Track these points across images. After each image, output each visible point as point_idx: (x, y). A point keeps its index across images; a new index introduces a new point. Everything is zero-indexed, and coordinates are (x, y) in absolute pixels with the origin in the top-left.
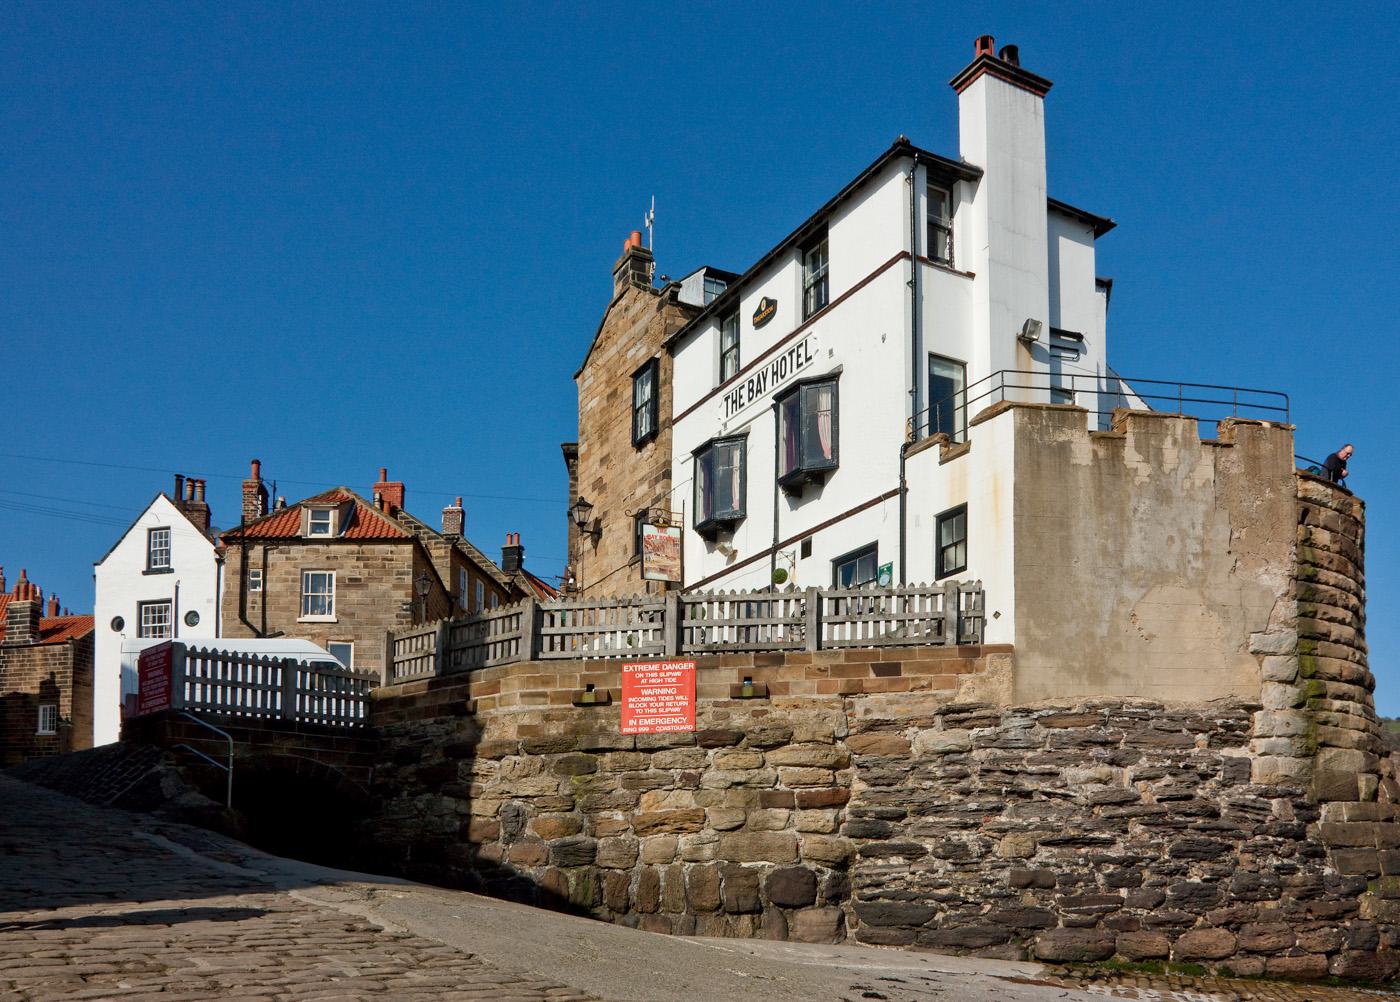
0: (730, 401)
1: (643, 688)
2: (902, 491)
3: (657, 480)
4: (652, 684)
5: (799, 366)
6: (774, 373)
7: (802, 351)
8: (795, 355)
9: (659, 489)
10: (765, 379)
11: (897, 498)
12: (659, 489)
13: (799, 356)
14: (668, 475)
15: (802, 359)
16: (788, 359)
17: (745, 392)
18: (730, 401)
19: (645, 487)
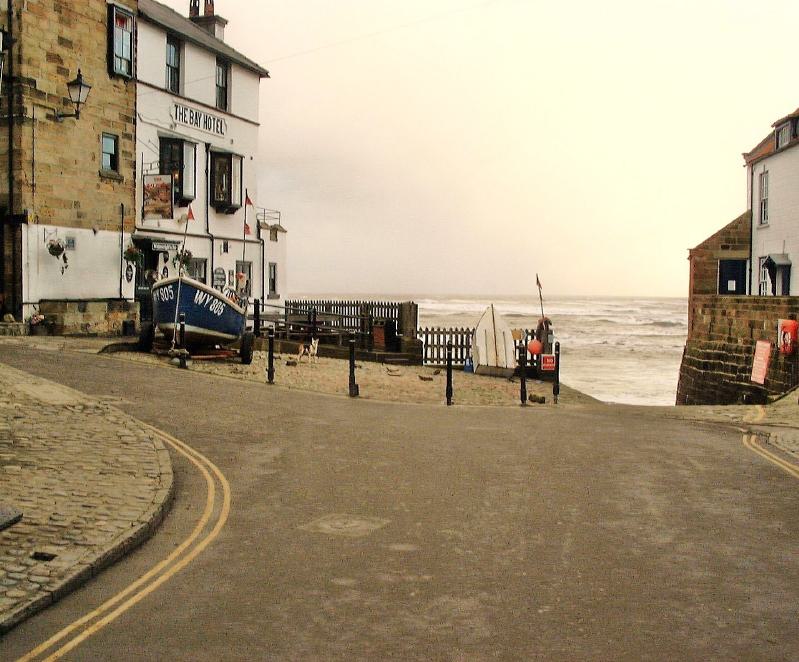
3: (127, 119)
12: (129, 131)
14: (135, 123)
17: (188, 113)
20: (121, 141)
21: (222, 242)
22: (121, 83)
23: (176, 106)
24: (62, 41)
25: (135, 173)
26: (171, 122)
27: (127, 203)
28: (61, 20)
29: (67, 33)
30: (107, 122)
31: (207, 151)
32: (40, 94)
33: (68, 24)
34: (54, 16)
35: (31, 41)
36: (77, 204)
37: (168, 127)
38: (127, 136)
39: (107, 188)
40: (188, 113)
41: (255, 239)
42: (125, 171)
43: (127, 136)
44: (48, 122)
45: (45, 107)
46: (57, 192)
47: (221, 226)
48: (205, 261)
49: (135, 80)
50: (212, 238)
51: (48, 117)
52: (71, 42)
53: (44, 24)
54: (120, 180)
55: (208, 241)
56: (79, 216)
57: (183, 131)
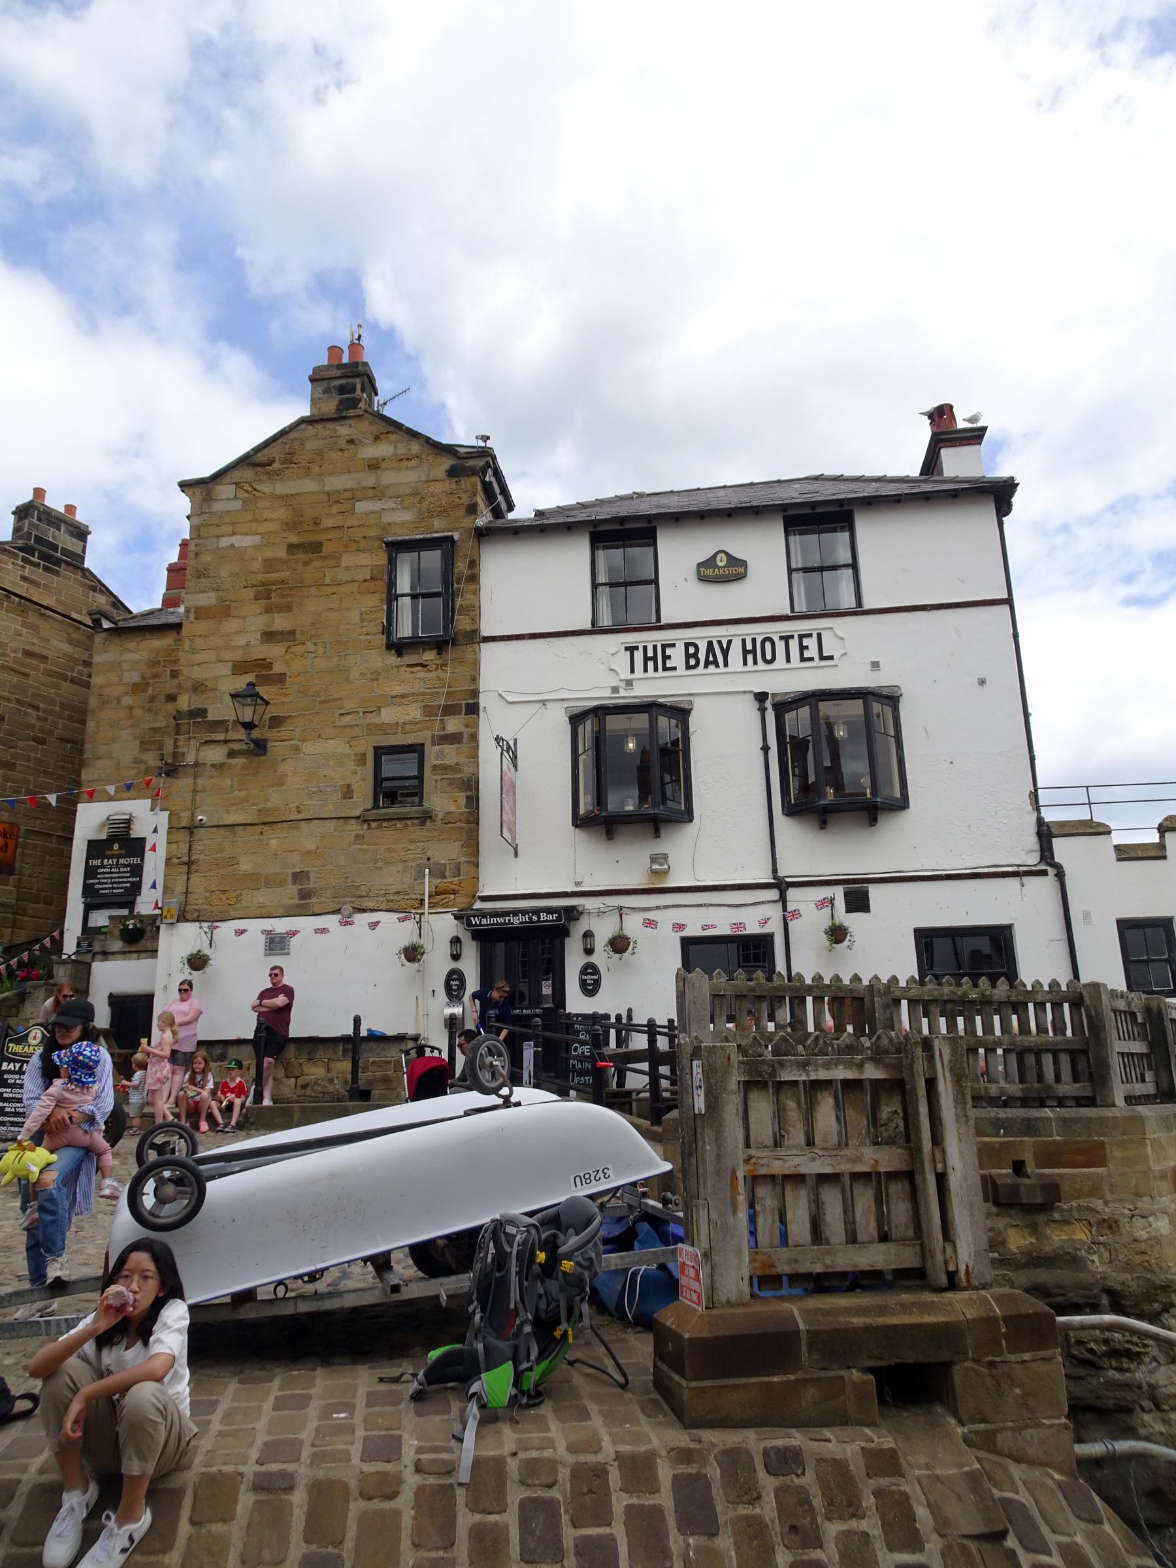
2: (1060, 875)
3: (449, 710)
5: (803, 659)
6: (745, 652)
7: (811, 643)
8: (794, 645)
9: (453, 725)
10: (725, 653)
12: (453, 725)
13: (803, 648)
14: (473, 709)
15: (813, 652)
16: (780, 646)
17: (677, 656)
18: (639, 656)
19: (414, 712)
20: (431, 752)
21: (839, 893)
22: (429, 656)
23: (632, 650)
24: (269, 636)
25: (473, 802)
26: (615, 682)
28: (268, 610)
29: (280, 622)
30: (383, 729)
31: (763, 710)
32: (219, 725)
33: (288, 608)
34: (257, 607)
35: (199, 658)
36: (298, 877)
37: (608, 693)
38: (454, 738)
39: (386, 839)
40: (677, 656)
42: (441, 800)
43: (454, 738)
44: (233, 761)
45: (226, 742)
46: (246, 865)
48: (768, 939)
49: (475, 638)
50: (781, 886)
51: (232, 754)
52: (292, 633)
53: (230, 626)
54: (426, 818)
56: (304, 895)
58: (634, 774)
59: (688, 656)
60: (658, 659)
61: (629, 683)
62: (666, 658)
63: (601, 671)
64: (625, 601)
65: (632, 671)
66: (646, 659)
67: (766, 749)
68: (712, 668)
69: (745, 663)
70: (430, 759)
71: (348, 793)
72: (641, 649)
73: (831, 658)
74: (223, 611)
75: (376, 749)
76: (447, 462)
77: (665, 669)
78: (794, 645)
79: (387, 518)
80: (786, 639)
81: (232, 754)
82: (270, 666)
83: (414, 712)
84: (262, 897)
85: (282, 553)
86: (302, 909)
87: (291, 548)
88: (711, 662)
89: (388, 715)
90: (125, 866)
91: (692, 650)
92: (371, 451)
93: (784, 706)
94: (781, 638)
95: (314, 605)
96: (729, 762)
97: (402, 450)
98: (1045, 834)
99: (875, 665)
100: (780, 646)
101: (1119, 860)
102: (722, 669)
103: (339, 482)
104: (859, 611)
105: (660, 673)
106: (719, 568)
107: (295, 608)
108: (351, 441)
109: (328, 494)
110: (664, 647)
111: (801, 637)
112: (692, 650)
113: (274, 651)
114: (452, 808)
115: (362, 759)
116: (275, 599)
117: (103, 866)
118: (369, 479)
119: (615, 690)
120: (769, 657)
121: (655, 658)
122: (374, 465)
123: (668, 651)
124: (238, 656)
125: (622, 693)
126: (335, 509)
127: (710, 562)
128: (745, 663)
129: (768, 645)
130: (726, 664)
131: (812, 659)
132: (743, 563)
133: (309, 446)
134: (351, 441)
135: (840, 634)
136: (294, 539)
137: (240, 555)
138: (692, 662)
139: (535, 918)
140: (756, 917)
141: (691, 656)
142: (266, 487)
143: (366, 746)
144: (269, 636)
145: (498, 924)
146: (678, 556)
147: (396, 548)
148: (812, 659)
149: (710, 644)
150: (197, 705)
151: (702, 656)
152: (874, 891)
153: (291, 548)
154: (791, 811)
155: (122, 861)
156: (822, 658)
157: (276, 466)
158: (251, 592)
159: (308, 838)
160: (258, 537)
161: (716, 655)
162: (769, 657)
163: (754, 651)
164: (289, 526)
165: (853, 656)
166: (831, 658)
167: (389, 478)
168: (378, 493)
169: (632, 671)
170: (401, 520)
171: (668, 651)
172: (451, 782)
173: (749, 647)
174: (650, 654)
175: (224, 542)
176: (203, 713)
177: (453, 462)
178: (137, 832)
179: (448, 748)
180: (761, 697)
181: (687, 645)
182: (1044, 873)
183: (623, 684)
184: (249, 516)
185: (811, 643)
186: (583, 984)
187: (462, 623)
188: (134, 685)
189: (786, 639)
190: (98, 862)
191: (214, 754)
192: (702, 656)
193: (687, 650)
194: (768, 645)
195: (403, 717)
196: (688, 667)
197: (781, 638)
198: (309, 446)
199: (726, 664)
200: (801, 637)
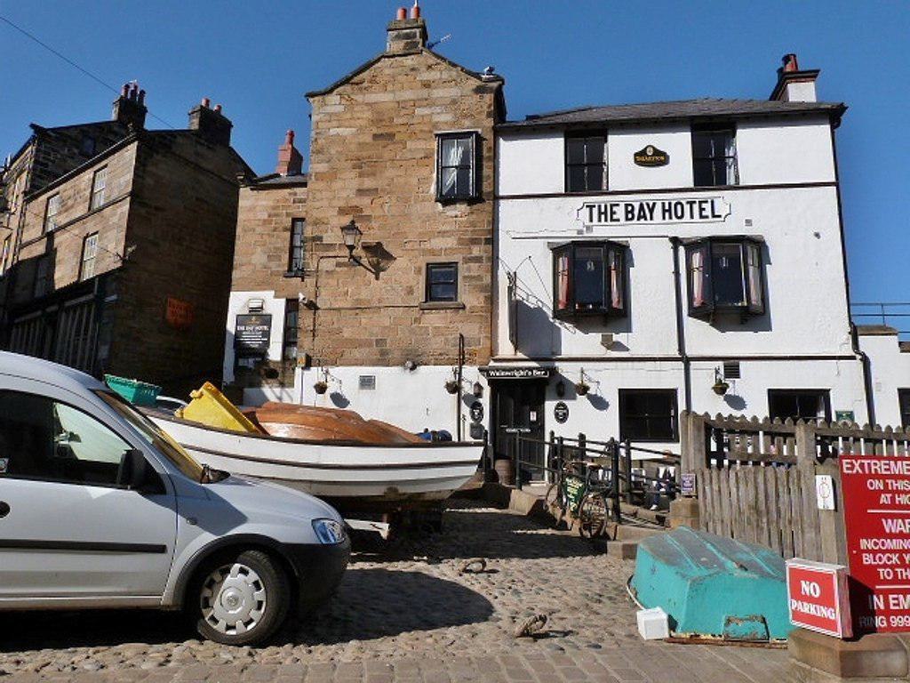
0: (595, 211)
1: (887, 516)
4: (901, 507)
5: (701, 217)
6: (664, 211)
7: (707, 206)
8: (696, 207)
10: (651, 211)
11: (857, 365)
13: (702, 210)
15: (708, 212)
16: (687, 208)
17: (620, 212)
18: (595, 211)
19: (451, 242)
24: (361, 192)
27: (472, 330)
28: (361, 175)
29: (368, 183)
30: (432, 252)
35: (318, 204)
36: (379, 342)
39: (434, 319)
40: (620, 212)
41: (851, 353)
42: (469, 296)
44: (338, 269)
45: (335, 257)
46: (346, 334)
47: (704, 338)
50: (687, 361)
53: (337, 185)
55: (681, 365)
56: (383, 353)
57: (603, 231)
58: (593, 285)
59: (627, 212)
60: (607, 214)
61: (588, 228)
62: (613, 213)
63: (572, 219)
64: (584, 176)
65: (591, 221)
66: (600, 213)
67: (677, 273)
68: (642, 221)
69: (664, 218)
70: (463, 271)
71: (410, 291)
72: (597, 207)
73: (719, 216)
74: (332, 175)
75: (428, 264)
76: (479, 83)
77: (612, 220)
78: (696, 207)
79: (436, 119)
80: (691, 203)
81: (338, 265)
82: (361, 210)
83: (451, 242)
84: (357, 353)
85: (368, 139)
86: (383, 360)
87: (375, 137)
88: (642, 216)
89: (438, 243)
90: (259, 331)
91: (630, 208)
92: (426, 76)
93: (692, 246)
94: (688, 203)
95: (390, 173)
96: (654, 283)
97: (445, 76)
98: (855, 334)
99: (748, 222)
100: (687, 208)
101: (902, 351)
102: (649, 221)
103: (408, 95)
104: (737, 187)
105: (609, 223)
106: (648, 156)
107: (378, 175)
108: (413, 69)
109: (398, 102)
110: (612, 206)
111: (700, 202)
112: (630, 208)
113: (365, 201)
114: (476, 303)
115: (419, 271)
116: (365, 168)
117: (245, 331)
118: (424, 93)
119: (580, 232)
120: (679, 214)
121: (605, 213)
122: (427, 85)
123: (615, 209)
124: (342, 204)
125: (585, 235)
126: (403, 112)
127: (643, 153)
128: (664, 218)
129: (679, 207)
130: (651, 219)
131: (707, 217)
132: (664, 154)
133: (387, 71)
134: (413, 69)
135: (723, 200)
136: (375, 131)
137: (343, 139)
138: (630, 216)
139: (530, 373)
140: (666, 377)
141: (629, 212)
142: (359, 98)
143: (422, 262)
144: (361, 192)
145: (508, 376)
146: (620, 150)
147: (444, 137)
148: (707, 217)
149: (641, 205)
150: (316, 234)
151: (636, 212)
152: (742, 364)
153: (375, 137)
154: (694, 313)
155: (257, 328)
156: (714, 216)
157: (365, 84)
158: (349, 164)
159: (385, 319)
160: (354, 130)
161: (645, 213)
162: (679, 214)
163: (669, 211)
164: (374, 122)
165: (732, 214)
166: (719, 216)
167: (437, 93)
168: (429, 102)
169: (591, 221)
170: (445, 120)
171: (615, 209)
172: (475, 287)
173: (667, 208)
174: (603, 210)
175: (332, 132)
176: (320, 239)
177: (479, 83)
178: (267, 311)
179: (474, 266)
180: (676, 241)
181: (627, 205)
182: (853, 358)
183: (585, 229)
184: (349, 116)
185: (707, 206)
186: (557, 415)
187: (486, 188)
188: (265, 221)
189: (691, 203)
190: (243, 328)
191: (327, 265)
192: (636, 212)
193: (626, 208)
194: (679, 207)
195: (445, 247)
196: (627, 219)
197: (688, 203)
198: (387, 71)
199: (651, 219)
200: (700, 202)
